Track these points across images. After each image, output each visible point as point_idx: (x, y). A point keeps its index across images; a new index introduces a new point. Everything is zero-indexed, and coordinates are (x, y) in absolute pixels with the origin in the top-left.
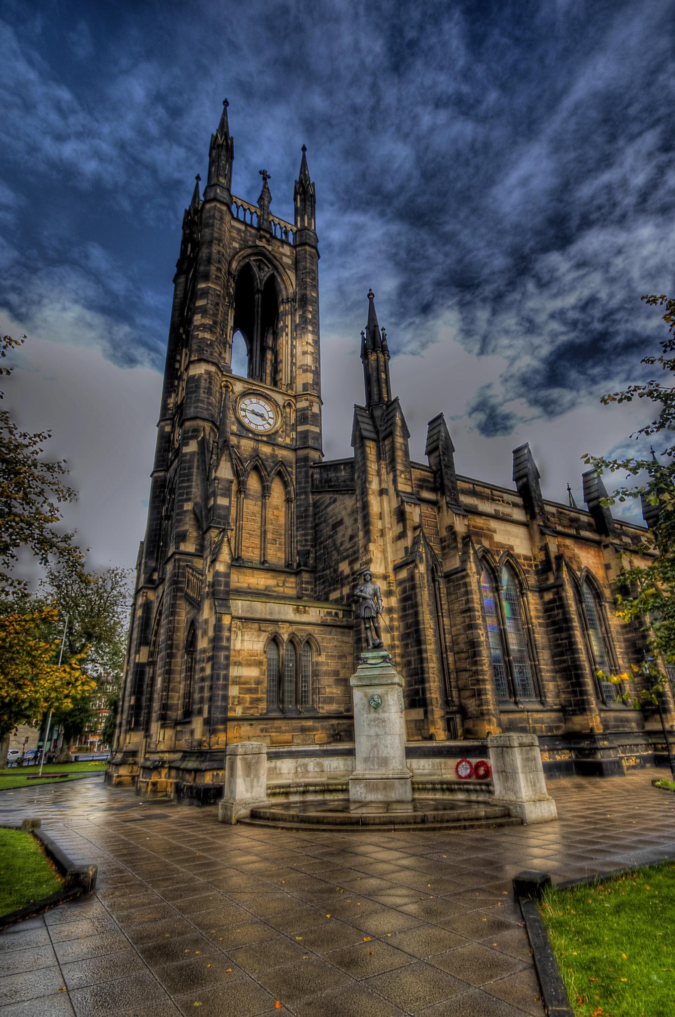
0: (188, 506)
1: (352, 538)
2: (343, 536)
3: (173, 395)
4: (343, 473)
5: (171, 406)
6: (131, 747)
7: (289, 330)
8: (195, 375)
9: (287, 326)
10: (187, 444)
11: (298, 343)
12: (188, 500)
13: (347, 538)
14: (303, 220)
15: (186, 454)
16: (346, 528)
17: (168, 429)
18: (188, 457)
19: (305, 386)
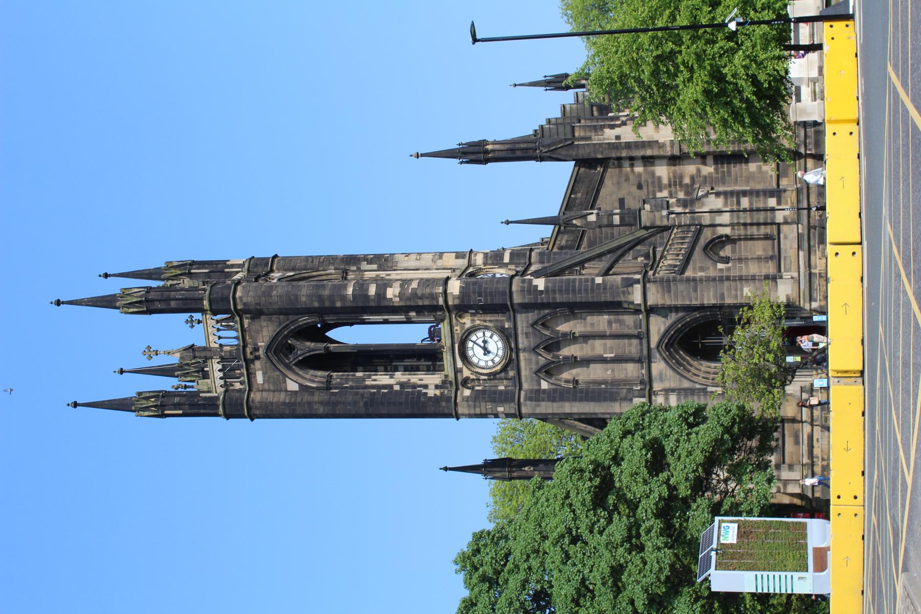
0: (599, 280)
1: (640, 187)
2: (634, 198)
3: (424, 391)
4: (579, 195)
5: (438, 392)
6: (799, 389)
7: (383, 274)
8: (461, 287)
9: (378, 276)
10: (536, 286)
11: (402, 265)
12: (593, 280)
13: (637, 192)
14: (233, 266)
15: (546, 287)
16: (629, 193)
17: (467, 393)
18: (550, 285)
19: (457, 257)
